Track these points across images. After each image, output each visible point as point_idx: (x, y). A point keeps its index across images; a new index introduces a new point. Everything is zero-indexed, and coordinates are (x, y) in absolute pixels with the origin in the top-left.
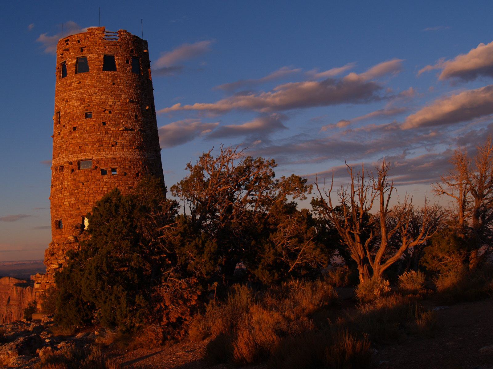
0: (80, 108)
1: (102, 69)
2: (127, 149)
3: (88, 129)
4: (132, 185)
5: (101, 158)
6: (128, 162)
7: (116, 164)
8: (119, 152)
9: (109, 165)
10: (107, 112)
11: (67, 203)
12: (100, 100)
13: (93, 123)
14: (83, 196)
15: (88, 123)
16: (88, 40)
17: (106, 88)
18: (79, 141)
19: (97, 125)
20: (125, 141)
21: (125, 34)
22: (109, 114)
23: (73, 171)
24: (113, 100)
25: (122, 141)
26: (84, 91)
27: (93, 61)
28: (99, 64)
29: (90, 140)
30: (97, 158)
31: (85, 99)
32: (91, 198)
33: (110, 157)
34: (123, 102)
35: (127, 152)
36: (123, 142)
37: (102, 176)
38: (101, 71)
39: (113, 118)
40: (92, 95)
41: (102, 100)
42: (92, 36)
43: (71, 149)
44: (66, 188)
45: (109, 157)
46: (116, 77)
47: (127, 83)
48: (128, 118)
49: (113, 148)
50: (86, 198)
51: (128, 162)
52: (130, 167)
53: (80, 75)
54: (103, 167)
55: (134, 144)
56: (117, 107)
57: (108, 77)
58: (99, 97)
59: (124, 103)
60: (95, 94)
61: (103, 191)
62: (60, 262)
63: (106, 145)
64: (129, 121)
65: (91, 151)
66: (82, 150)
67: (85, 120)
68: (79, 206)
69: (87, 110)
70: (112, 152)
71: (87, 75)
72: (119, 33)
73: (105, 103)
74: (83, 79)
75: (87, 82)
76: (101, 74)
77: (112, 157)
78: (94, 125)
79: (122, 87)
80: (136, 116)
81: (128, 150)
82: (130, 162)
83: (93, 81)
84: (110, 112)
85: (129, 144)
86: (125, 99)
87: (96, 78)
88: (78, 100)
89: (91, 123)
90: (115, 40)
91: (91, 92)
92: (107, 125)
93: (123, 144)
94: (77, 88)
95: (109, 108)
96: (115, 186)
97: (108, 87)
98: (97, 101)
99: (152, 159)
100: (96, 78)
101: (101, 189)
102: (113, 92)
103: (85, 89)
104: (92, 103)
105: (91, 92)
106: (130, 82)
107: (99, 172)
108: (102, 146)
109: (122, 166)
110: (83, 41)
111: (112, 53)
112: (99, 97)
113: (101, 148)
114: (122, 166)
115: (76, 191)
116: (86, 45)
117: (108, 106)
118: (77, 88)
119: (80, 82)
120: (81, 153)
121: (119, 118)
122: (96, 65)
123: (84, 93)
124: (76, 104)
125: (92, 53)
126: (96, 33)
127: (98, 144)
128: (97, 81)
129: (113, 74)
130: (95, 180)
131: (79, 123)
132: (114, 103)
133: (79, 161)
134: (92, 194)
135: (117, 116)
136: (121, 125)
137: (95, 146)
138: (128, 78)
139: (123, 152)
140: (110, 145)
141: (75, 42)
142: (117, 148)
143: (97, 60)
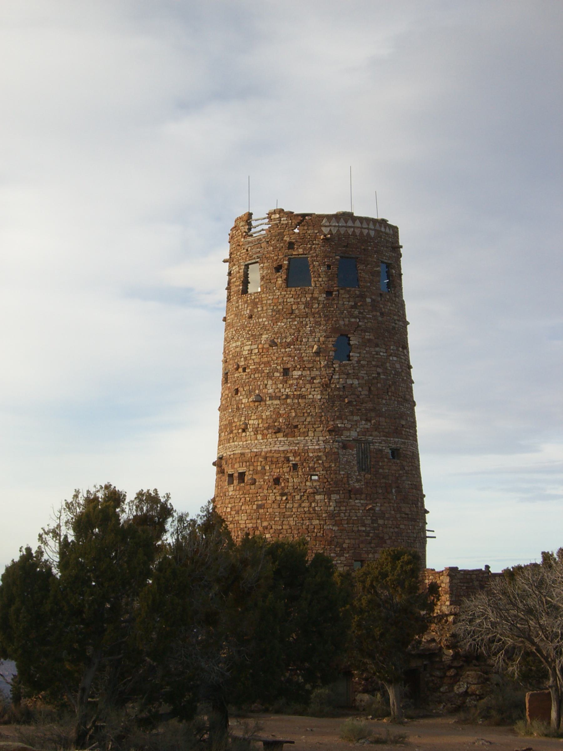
2: (263, 434)
4: (264, 502)
6: (260, 459)
9: (236, 466)
10: (241, 370)
19: (230, 395)
21: (278, 216)
22: (243, 374)
25: (255, 421)
34: (263, 348)
35: (262, 441)
36: (256, 422)
38: (240, 296)
39: (247, 380)
45: (236, 452)
46: (256, 304)
47: (273, 310)
48: (269, 376)
49: (244, 434)
51: (260, 459)
52: (263, 468)
55: (276, 424)
56: (253, 360)
57: (246, 305)
59: (264, 350)
61: (227, 514)
64: (270, 382)
70: (241, 443)
72: (270, 215)
77: (240, 452)
79: (264, 319)
80: (286, 372)
82: (266, 458)
84: (244, 370)
85: (266, 425)
92: (239, 394)
93: (256, 426)
95: (242, 363)
98: (233, 351)
99: (317, 447)
102: (250, 332)
106: (280, 307)
108: (231, 432)
109: (251, 468)
111: (254, 258)
113: (231, 436)
117: (242, 359)
121: (255, 378)
129: (253, 297)
135: (252, 376)
139: (256, 442)
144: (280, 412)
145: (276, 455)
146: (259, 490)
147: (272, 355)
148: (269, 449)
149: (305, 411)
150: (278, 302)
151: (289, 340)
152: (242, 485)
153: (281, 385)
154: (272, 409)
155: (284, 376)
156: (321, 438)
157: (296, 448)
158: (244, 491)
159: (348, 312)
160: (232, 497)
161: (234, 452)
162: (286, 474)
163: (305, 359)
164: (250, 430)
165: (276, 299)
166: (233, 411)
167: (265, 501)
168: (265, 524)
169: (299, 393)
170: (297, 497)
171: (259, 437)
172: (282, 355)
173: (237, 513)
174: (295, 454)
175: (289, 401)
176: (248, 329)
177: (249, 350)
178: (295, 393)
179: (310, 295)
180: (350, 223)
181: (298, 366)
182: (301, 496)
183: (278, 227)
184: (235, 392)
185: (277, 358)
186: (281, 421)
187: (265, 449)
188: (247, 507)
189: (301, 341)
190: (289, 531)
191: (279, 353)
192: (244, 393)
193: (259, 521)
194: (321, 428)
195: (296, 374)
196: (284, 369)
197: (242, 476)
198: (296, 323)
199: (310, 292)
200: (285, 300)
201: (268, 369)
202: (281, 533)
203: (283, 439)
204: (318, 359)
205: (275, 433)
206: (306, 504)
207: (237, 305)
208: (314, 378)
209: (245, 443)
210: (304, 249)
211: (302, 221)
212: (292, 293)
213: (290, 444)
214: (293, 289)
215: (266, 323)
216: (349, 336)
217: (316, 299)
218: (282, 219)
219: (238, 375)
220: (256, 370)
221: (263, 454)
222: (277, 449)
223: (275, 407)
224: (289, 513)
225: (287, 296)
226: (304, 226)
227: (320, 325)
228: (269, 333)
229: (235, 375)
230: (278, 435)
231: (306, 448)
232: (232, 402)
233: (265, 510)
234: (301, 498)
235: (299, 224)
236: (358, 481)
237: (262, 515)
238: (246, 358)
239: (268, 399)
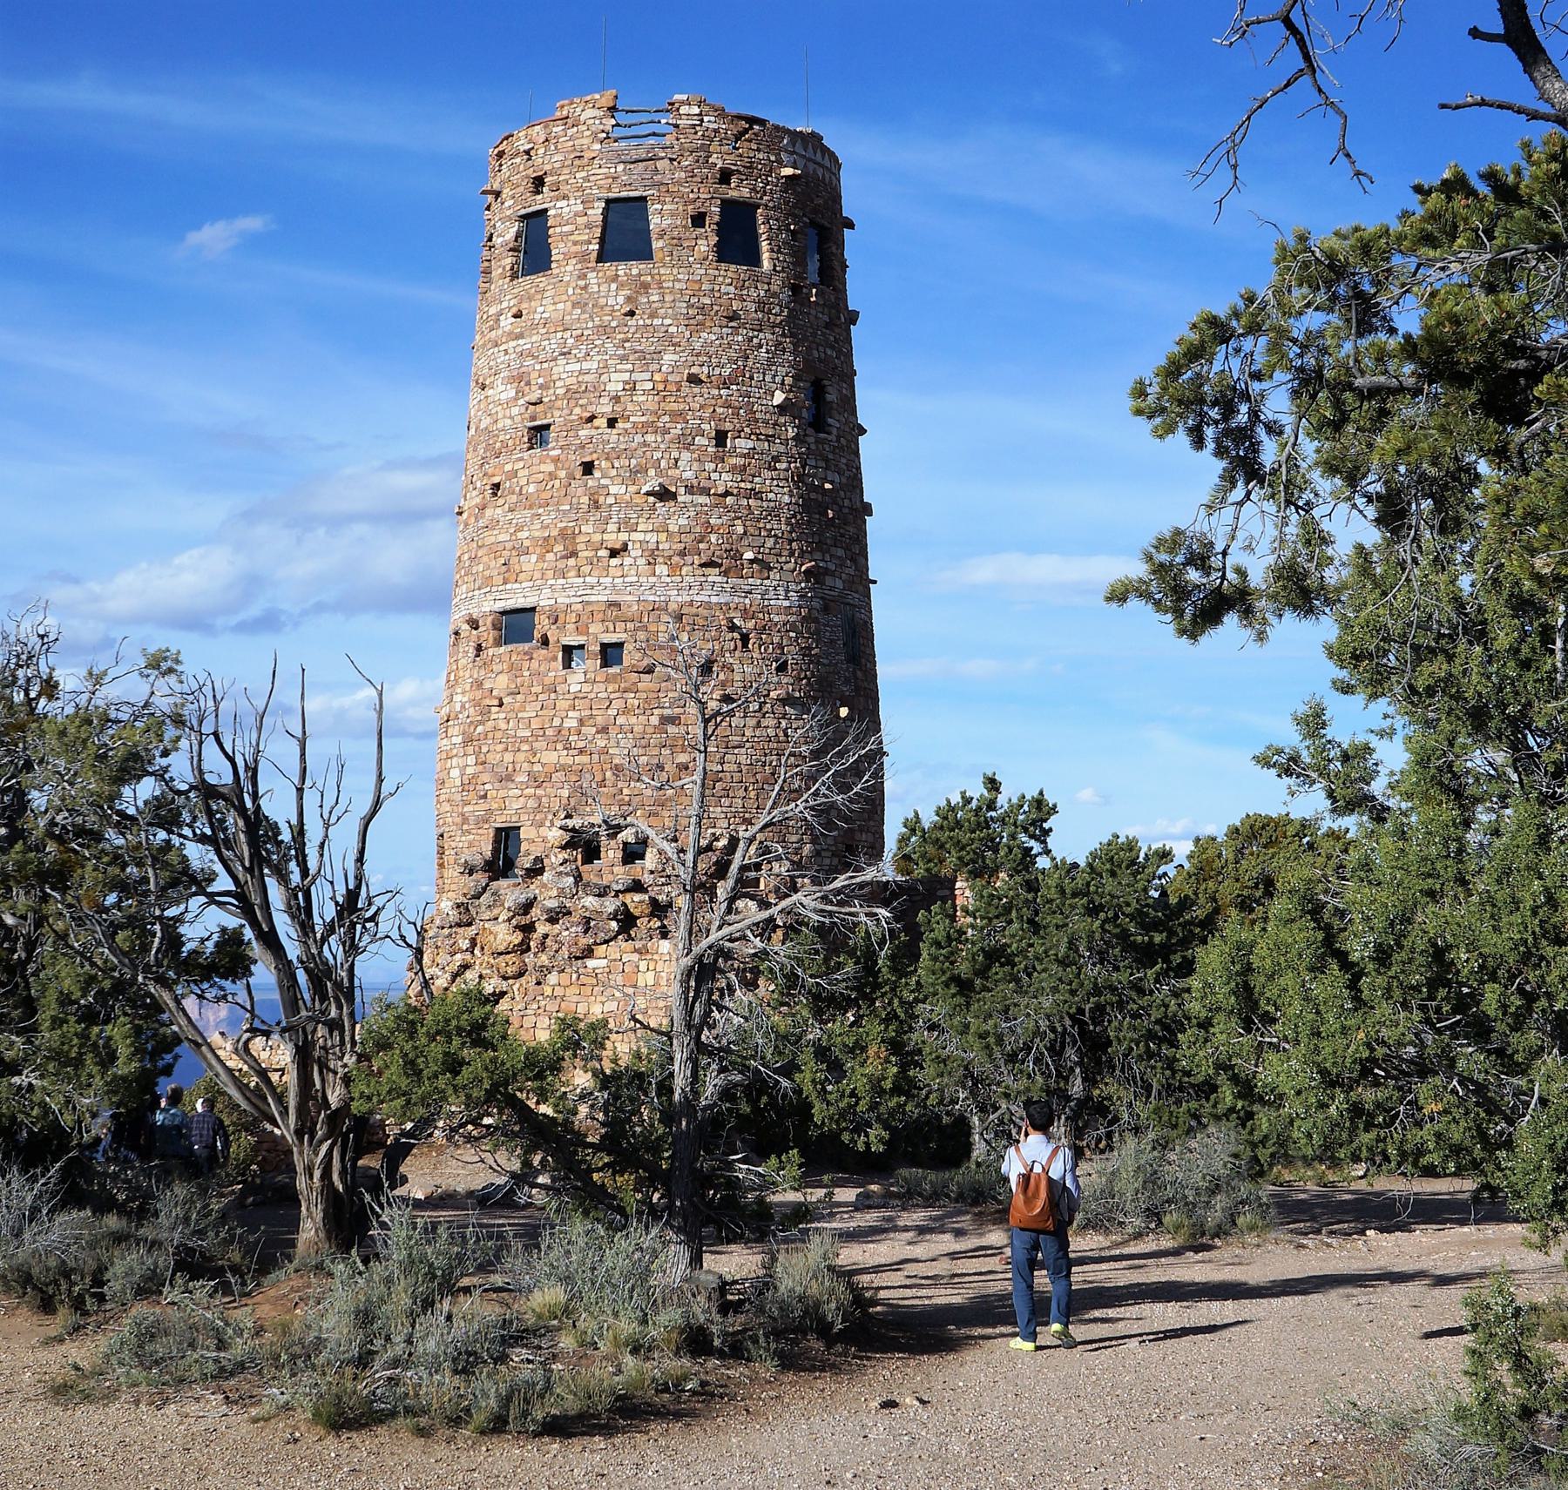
0: (515, 411)
1: (595, 255)
3: (532, 489)
5: (567, 601)
7: (620, 626)
8: (636, 579)
10: (601, 422)
12: (580, 379)
13: (550, 467)
14: (500, 747)
15: (535, 469)
16: (556, 148)
17: (605, 330)
18: (502, 538)
19: (562, 474)
20: (663, 537)
21: (696, 110)
23: (479, 648)
24: (626, 376)
26: (529, 346)
27: (565, 229)
28: (586, 237)
29: (537, 534)
30: (553, 602)
31: (534, 375)
32: (521, 757)
33: (600, 598)
35: (668, 580)
37: (564, 672)
39: (623, 447)
40: (555, 359)
41: (587, 378)
42: (570, 132)
43: (481, 568)
45: (593, 598)
46: (646, 286)
48: (685, 442)
49: (614, 562)
50: (508, 757)
51: (665, 618)
53: (525, 283)
54: (572, 640)
55: (701, 546)
57: (614, 286)
58: (577, 367)
60: (564, 354)
63: (586, 554)
64: (686, 455)
65: (537, 575)
66: (510, 573)
67: (526, 455)
68: (487, 787)
69: (533, 419)
71: (540, 280)
73: (598, 390)
74: (530, 299)
75: (544, 309)
76: (589, 275)
78: (552, 476)
79: (668, 321)
80: (721, 438)
81: (674, 570)
82: (679, 617)
83: (561, 306)
84: (612, 423)
85: (681, 546)
86: (675, 367)
87: (570, 291)
89: (543, 468)
90: (652, 141)
92: (597, 474)
95: (608, 409)
96: (610, 712)
97: (614, 324)
99: (787, 603)
100: (570, 291)
101: (557, 722)
102: (627, 345)
103: (534, 338)
104: (551, 391)
105: (552, 345)
106: (707, 301)
107: (555, 659)
108: (574, 554)
109: (641, 635)
110: (541, 151)
112: (577, 367)
113: (572, 562)
114: (641, 635)
115: (479, 729)
116: (547, 167)
119: (518, 315)
120: (505, 583)
121: (645, 444)
122: (575, 243)
124: (503, 396)
125: (565, 197)
126: (582, 118)
127: (559, 548)
128: (575, 305)
129: (635, 272)
130: (539, 689)
131: (508, 467)
132: (631, 387)
133: (503, 613)
134: (524, 740)
136: (652, 472)
137: (550, 556)
138: (697, 287)
140: (603, 553)
141: (518, 160)
142: (628, 561)
143: (581, 220)
144: (711, 521)
145: (706, 613)
146: (663, 684)
147: (689, 400)
148: (688, 599)
149: (762, 525)
150: (700, 289)
151: (727, 372)
152: (611, 670)
153: (713, 466)
154: (693, 514)
155: (717, 446)
156: (792, 586)
157: (747, 601)
158: (622, 685)
159: (823, 334)
160: (581, 695)
161: (586, 598)
162: (727, 655)
163: (758, 415)
164: (633, 553)
165: (696, 282)
167: (682, 710)
168: (682, 758)
169: (749, 486)
170: (754, 706)
171: (662, 569)
172: (713, 402)
173: (604, 730)
174: (746, 614)
175: (729, 500)
176: (622, 336)
177: (626, 383)
178: (742, 485)
179: (766, 287)
180: (819, 157)
181: (747, 430)
182: (761, 703)
183: (696, 133)
184: (581, 468)
185: (702, 407)
186: (713, 540)
187: (677, 599)
188: (633, 720)
189: (751, 378)
190: (737, 776)
191: (706, 396)
192: (614, 472)
193: (665, 752)
194: (791, 566)
195: (743, 444)
196: (718, 432)
197: (610, 654)
198: (740, 338)
199: (766, 280)
200: (717, 288)
201: (679, 426)
202: (721, 780)
203: (719, 579)
204: (782, 420)
205: (702, 565)
206: (769, 721)
207: (582, 283)
208: (776, 459)
209: (617, 581)
210: (754, 190)
211: (746, 131)
212: (730, 274)
214: (733, 267)
215: (673, 329)
216: (826, 382)
217: (775, 295)
218: (706, 119)
219: (594, 432)
220: (645, 428)
221: (673, 607)
222: (706, 599)
223: (699, 509)
224: (739, 738)
225: (721, 279)
226: (750, 141)
227: (784, 350)
228: (683, 351)
229: (580, 433)
230: (708, 571)
231: (766, 603)
232: (571, 490)
233: (682, 729)
234: (760, 708)
235: (738, 138)
236: (847, 681)
237: (675, 738)
239: (682, 490)
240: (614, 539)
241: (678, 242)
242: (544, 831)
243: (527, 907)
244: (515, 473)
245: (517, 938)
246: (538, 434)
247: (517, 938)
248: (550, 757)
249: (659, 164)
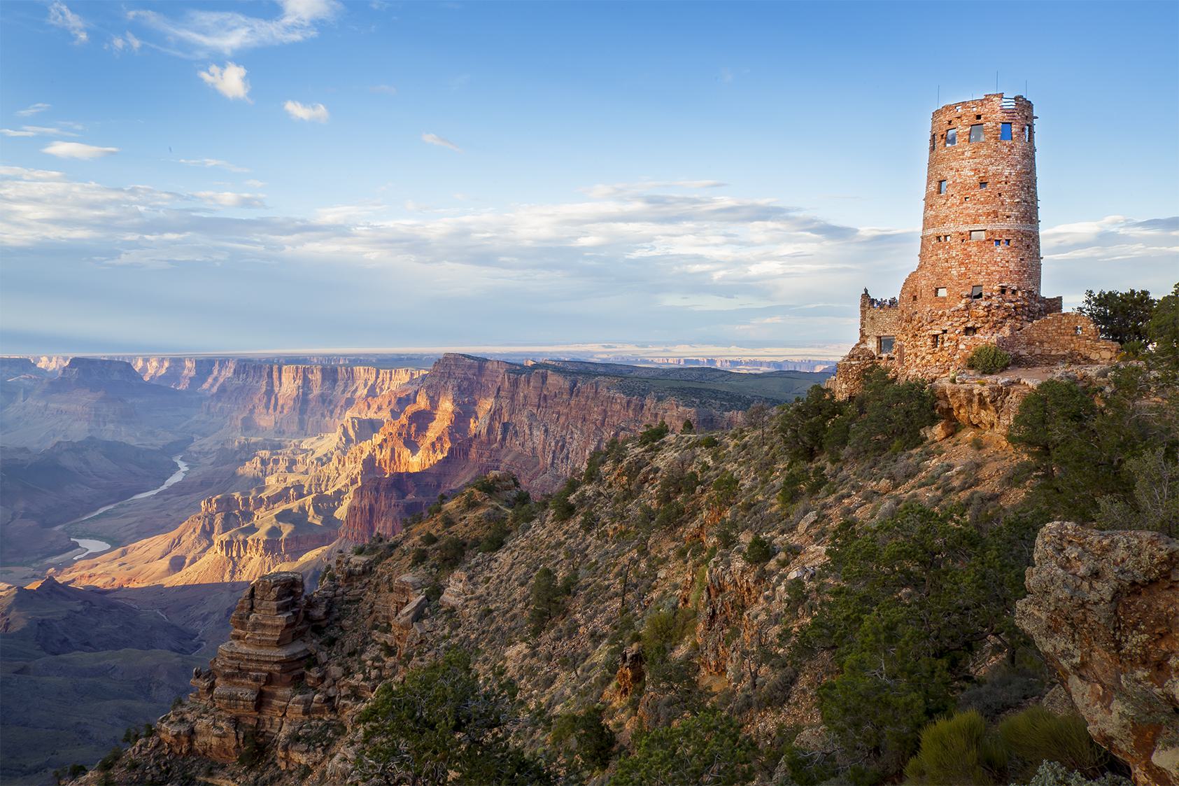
11: (954, 272)
44: (953, 257)
62: (946, 328)
73: (1001, 174)
78: (989, 196)
81: (1021, 221)
84: (1006, 183)
88: (971, 170)
91: (987, 161)
94: (970, 158)
118: (970, 158)
123: (979, 163)
132: (1010, 174)
166: (997, 205)
173: (1007, 262)
213: (1032, 227)
238: (1007, 177)
240: (1008, 213)
241: (1019, 136)
242: (991, 287)
243: (991, 305)
244: (975, 195)
245: (987, 314)
246: (983, 184)
247: (987, 314)
248: (994, 268)
249: (1016, 114)
